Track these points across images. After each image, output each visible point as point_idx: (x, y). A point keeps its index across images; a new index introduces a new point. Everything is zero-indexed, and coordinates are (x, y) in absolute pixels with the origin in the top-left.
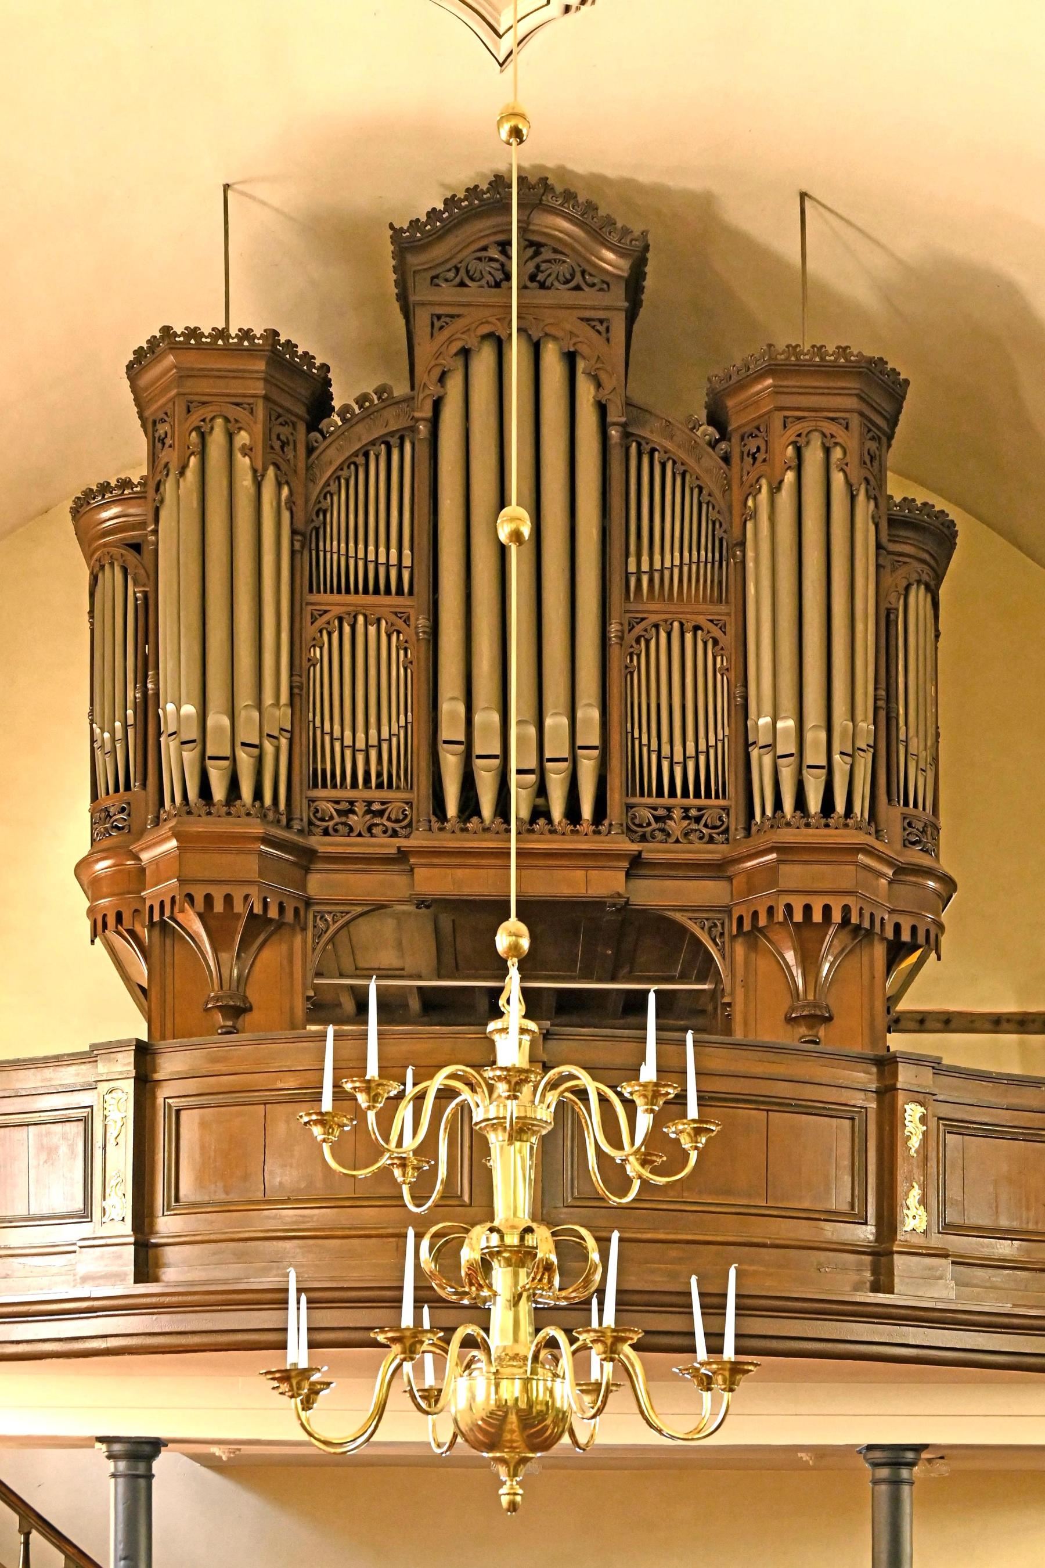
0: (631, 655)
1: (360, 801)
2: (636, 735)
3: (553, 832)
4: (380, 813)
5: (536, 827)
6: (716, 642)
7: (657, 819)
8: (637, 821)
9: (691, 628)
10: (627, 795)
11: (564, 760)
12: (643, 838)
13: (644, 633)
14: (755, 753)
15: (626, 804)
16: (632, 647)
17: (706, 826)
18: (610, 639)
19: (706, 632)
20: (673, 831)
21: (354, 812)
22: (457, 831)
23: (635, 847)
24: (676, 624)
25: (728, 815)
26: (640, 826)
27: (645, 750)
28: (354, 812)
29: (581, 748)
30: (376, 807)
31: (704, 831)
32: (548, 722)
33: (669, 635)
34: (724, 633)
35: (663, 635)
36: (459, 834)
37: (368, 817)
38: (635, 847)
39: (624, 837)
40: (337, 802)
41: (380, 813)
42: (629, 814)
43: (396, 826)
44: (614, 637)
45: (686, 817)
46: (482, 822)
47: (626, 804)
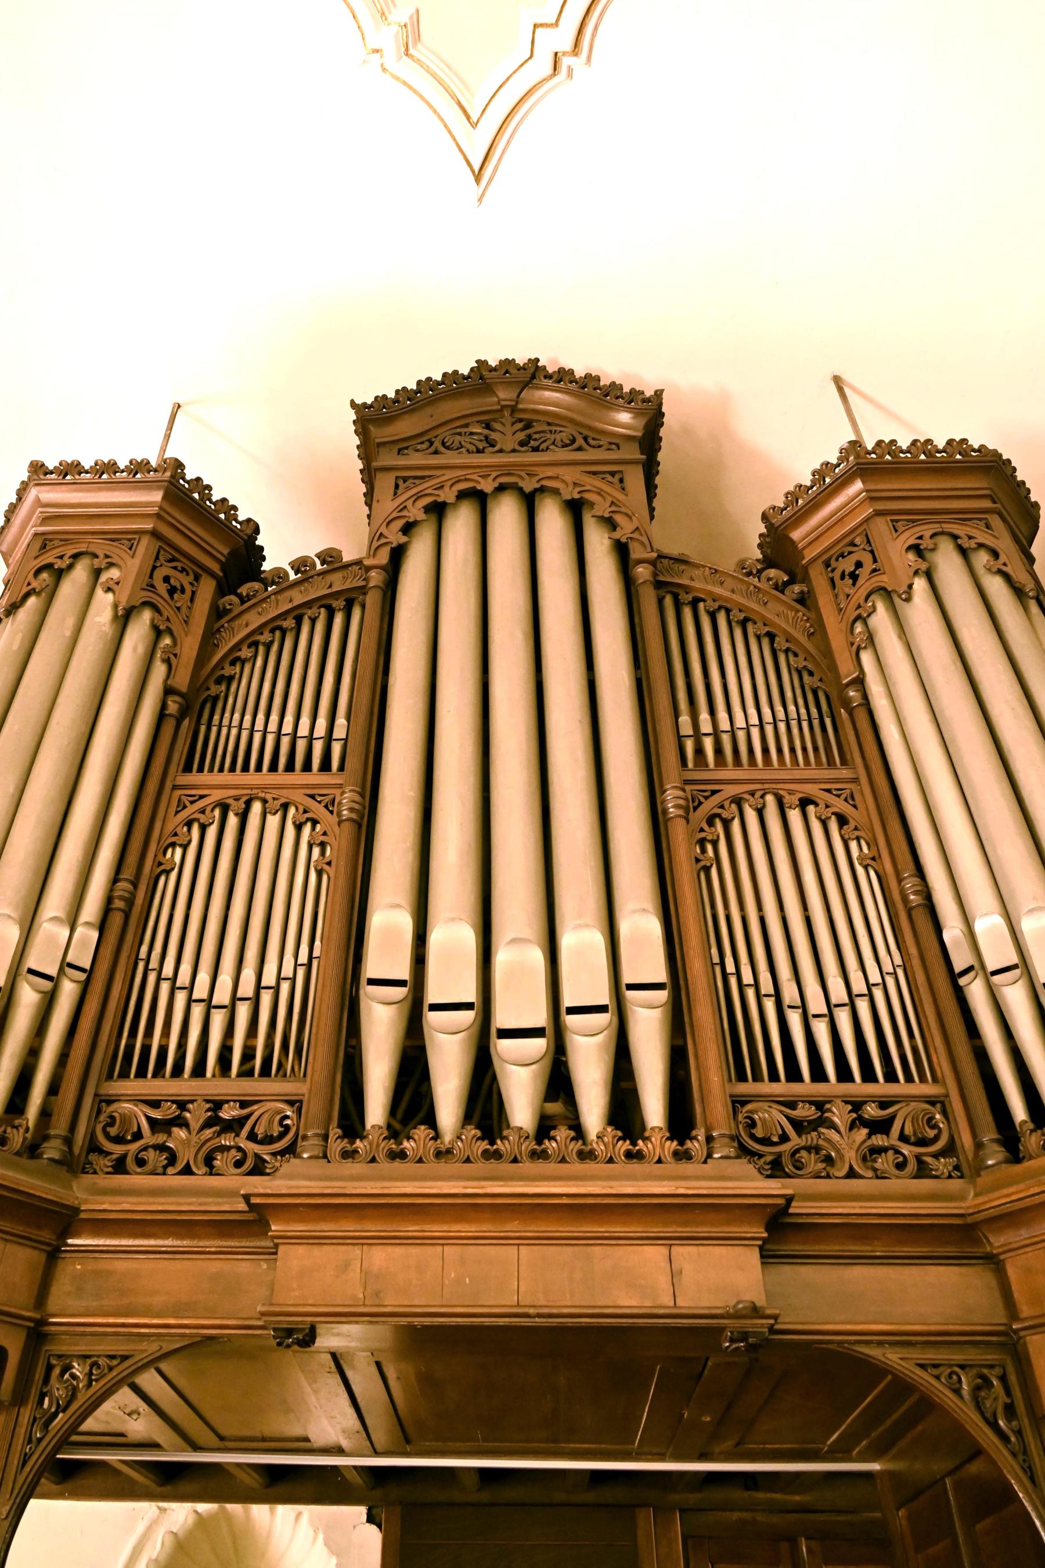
0: (702, 842)
2: (730, 968)
3: (586, 1155)
4: (233, 1126)
5: (551, 1146)
6: (842, 821)
7: (798, 1125)
8: (759, 1132)
9: (798, 803)
10: (730, 1080)
11: (602, 1009)
12: (776, 1169)
13: (719, 811)
14: (976, 992)
15: (731, 1096)
16: (702, 830)
17: (903, 1138)
18: (665, 811)
19: (822, 806)
20: (838, 1151)
21: (185, 1124)
22: (381, 1156)
23: (775, 1187)
24: (770, 799)
25: (944, 1113)
26: (766, 1141)
27: (750, 993)
28: (185, 1124)
29: (631, 987)
30: (228, 1113)
31: (906, 1149)
32: (567, 941)
33: (760, 813)
34: (855, 806)
35: (751, 816)
37: (208, 1132)
38: (775, 1187)
39: (744, 1166)
40: (155, 1104)
41: (233, 1126)
42: (740, 1117)
43: (263, 1151)
44: (672, 807)
45: (862, 1122)
46: (437, 1137)
47: (731, 1096)
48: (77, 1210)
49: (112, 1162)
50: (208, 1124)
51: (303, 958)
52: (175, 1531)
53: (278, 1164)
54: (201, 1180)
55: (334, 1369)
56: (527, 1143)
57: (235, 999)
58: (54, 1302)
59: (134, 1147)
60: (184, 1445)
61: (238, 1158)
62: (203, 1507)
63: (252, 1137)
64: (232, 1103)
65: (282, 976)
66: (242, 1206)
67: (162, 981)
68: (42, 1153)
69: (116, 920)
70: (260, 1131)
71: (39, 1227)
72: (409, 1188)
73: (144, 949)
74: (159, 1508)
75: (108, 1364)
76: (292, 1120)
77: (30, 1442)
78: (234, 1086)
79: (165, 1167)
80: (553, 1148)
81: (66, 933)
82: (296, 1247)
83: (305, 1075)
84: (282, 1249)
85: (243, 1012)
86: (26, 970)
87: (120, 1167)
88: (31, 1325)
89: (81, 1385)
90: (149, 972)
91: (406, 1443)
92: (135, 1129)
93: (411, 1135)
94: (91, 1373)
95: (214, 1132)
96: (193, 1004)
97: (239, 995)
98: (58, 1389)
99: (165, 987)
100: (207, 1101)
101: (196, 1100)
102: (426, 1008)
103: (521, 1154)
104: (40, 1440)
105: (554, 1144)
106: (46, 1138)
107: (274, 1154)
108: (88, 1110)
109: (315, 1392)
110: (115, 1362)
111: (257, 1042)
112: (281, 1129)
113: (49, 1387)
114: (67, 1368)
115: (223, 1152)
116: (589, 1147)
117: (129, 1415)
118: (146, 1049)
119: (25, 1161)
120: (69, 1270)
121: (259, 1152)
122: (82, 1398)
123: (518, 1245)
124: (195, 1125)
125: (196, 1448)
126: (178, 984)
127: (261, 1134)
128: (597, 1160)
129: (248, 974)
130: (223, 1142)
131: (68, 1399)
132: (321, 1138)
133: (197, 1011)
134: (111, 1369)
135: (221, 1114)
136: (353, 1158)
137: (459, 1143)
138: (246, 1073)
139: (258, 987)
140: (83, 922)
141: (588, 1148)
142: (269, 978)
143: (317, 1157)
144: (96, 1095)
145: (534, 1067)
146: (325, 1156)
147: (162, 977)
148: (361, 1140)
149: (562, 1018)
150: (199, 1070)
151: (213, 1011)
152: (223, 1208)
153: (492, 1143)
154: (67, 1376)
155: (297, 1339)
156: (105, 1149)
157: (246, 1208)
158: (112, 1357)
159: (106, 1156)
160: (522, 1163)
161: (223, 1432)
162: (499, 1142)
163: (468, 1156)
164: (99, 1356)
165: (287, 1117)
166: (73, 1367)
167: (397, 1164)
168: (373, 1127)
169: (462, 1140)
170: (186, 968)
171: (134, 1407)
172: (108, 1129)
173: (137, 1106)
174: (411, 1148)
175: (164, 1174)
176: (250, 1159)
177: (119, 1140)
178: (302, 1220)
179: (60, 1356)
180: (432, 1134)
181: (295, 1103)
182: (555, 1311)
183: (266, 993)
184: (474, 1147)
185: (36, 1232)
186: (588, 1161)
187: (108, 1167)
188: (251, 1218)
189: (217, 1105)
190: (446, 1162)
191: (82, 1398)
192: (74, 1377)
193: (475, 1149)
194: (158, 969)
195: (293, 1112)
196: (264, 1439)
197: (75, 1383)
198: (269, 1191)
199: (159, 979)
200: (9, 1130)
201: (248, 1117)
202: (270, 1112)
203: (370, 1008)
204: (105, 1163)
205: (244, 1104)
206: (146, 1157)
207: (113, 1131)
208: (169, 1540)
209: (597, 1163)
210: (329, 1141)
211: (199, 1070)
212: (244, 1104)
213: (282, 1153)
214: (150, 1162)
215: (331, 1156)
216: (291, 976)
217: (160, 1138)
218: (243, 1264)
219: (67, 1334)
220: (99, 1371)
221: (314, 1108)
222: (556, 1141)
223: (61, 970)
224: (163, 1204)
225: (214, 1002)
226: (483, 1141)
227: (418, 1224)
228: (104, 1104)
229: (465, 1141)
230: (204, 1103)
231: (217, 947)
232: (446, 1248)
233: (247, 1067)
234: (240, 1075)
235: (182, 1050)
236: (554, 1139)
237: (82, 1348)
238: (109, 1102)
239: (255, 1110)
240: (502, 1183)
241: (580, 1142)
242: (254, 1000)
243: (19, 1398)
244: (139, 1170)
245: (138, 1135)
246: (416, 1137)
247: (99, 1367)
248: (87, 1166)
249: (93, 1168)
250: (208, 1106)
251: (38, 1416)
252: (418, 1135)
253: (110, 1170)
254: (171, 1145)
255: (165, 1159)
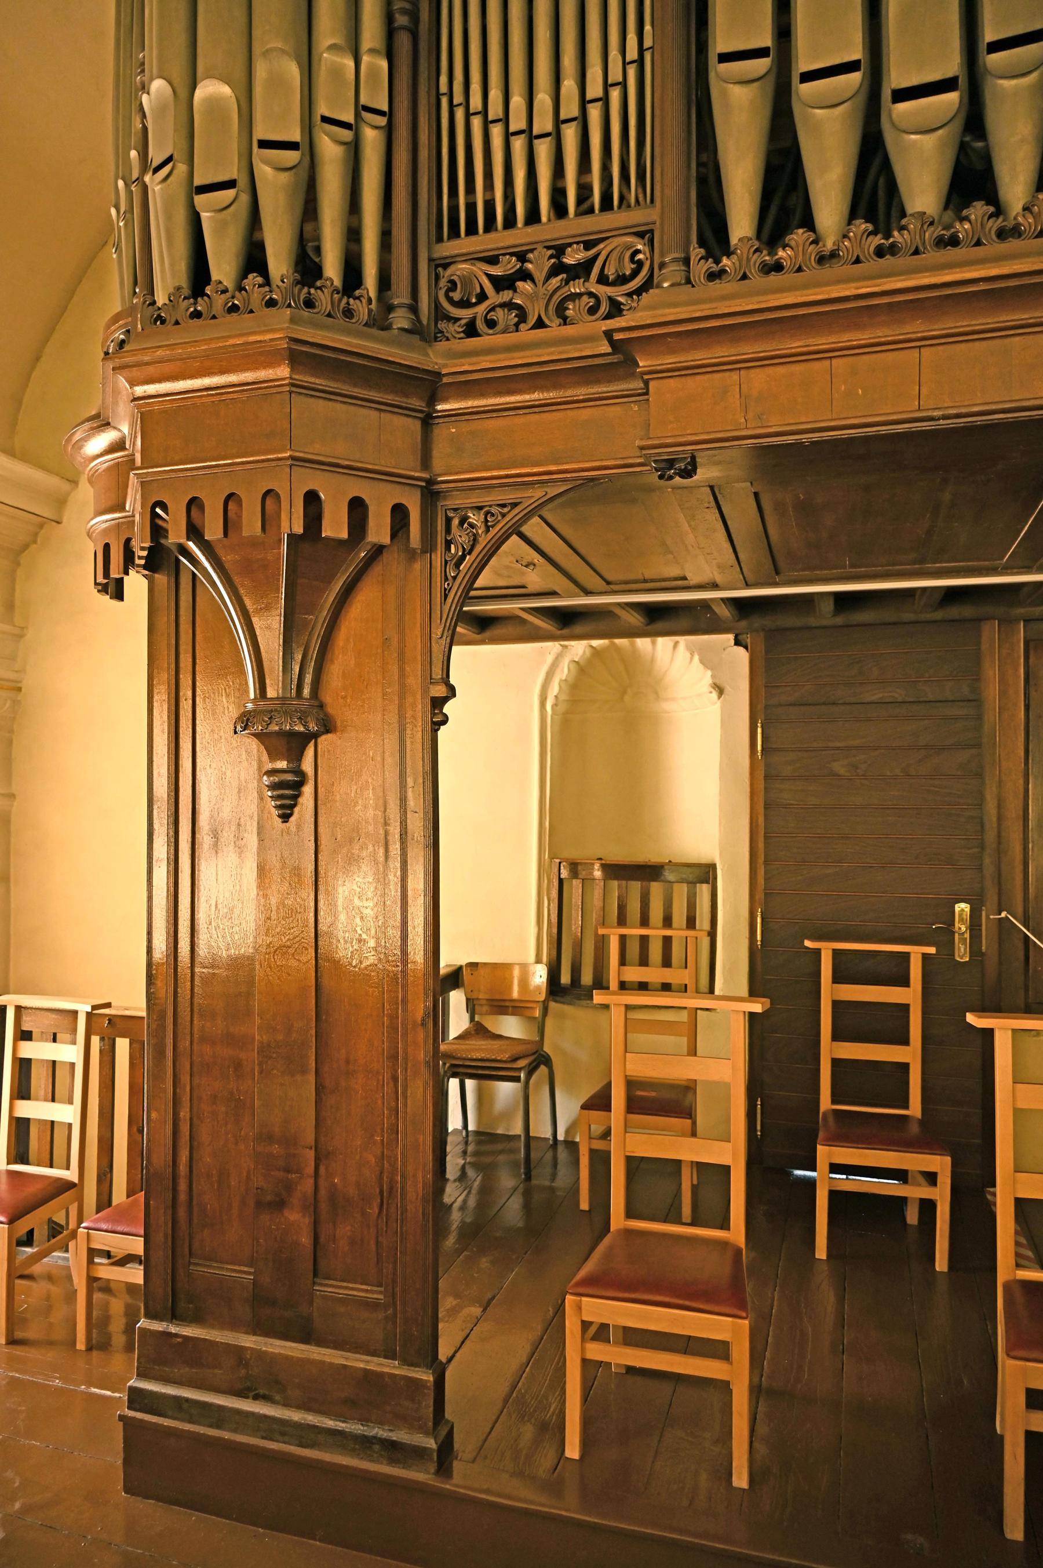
1: (539, 247)
4: (583, 269)
21: (526, 276)
22: (753, 272)
28: (526, 276)
30: (572, 258)
36: (757, 280)
37: (555, 281)
40: (493, 260)
41: (583, 269)
43: (617, 292)
48: (438, 375)
49: (462, 327)
50: (554, 272)
51: (632, 53)
52: (577, 660)
53: (634, 305)
54: (555, 329)
55: (713, 504)
56: (932, 229)
57: (559, 122)
58: (438, 463)
59: (481, 309)
60: (577, 590)
61: (591, 304)
62: (595, 643)
63: (602, 280)
64: (575, 246)
65: (610, 81)
66: (606, 348)
67: (472, 117)
68: (391, 324)
69: (403, 41)
70: (611, 272)
71: (406, 396)
72: (790, 299)
73: (444, 79)
74: (561, 645)
75: (500, 513)
76: (645, 254)
77: (446, 579)
78: (574, 225)
79: (517, 325)
80: (966, 230)
81: (351, 64)
82: (667, 380)
83: (652, 201)
84: (652, 384)
85: (570, 135)
86: (319, 118)
87: (471, 331)
88: (424, 484)
89: (480, 532)
90: (455, 108)
91: (776, 573)
92: (478, 290)
93: (787, 242)
94: (486, 521)
95: (562, 280)
96: (512, 138)
97: (563, 116)
98: (460, 536)
99: (476, 122)
100: (548, 248)
101: (535, 249)
102: (795, 78)
103: (924, 243)
104: (454, 578)
105: (967, 226)
106: (390, 308)
107: (629, 295)
108: (426, 277)
109: (694, 529)
110: (506, 510)
111: (592, 178)
112: (633, 266)
113: (452, 536)
114: (463, 520)
115: (574, 301)
116: (1013, 223)
117: (526, 566)
118: (471, 207)
119: (374, 331)
120: (443, 434)
121: (612, 294)
122: (483, 541)
123: (920, 347)
124: (540, 276)
125: (588, 593)
126: (490, 118)
127: (613, 274)
128: (1022, 238)
129: (569, 85)
130: (573, 291)
131: (471, 543)
132: (681, 263)
133: (518, 145)
134: (504, 515)
135: (565, 260)
136: (720, 279)
137: (846, 243)
138: (585, 208)
139: (584, 103)
140: (366, 49)
141: (1010, 224)
142: (595, 90)
143: (679, 284)
144: (431, 260)
145: (940, 132)
146: (688, 281)
147: (471, 111)
148: (728, 257)
149: (981, 62)
150: (533, 216)
151: (536, 142)
152: (584, 354)
153: (888, 235)
154: (466, 525)
155: (680, 469)
156: (452, 315)
157: (609, 350)
158: (503, 506)
159: (454, 323)
160: (924, 253)
161: (609, 578)
162: (896, 233)
163: (858, 256)
164: (490, 506)
165: (638, 252)
166: (470, 517)
167: (774, 278)
168: (740, 240)
169: (849, 239)
170: (495, 94)
171: (530, 560)
172: (451, 294)
173: (472, 264)
174: (788, 257)
175: (517, 331)
176: (605, 304)
177: (464, 304)
178: (673, 352)
179: (455, 510)
180: (812, 237)
181: (645, 234)
182: (964, 410)
183: (595, 108)
184: (865, 244)
185: (405, 400)
186: (1010, 239)
187: (459, 333)
188: (615, 361)
189: (559, 251)
190: (830, 267)
191: (483, 541)
192: (472, 526)
193: (866, 247)
194: (464, 103)
195: (645, 244)
196: (645, 581)
197: (474, 531)
198: (633, 324)
199: (468, 115)
200: (351, 301)
201: (595, 258)
202: (619, 248)
203: (724, 94)
204: (454, 329)
205: (588, 245)
206: (495, 318)
207: (456, 296)
208: (573, 666)
209: (1023, 240)
210: (692, 263)
211: (533, 216)
212: (588, 245)
213: (639, 291)
214: (501, 322)
215: (695, 281)
216: (621, 80)
217: (506, 296)
218: (613, 409)
219: (458, 490)
220: (494, 518)
221: (668, 233)
222: (970, 222)
223: (357, 115)
224: (523, 357)
225: (536, 131)
226: (876, 235)
227: (799, 340)
228: (440, 269)
229: (853, 240)
230: (545, 250)
231: (526, 63)
232: (834, 361)
233: (585, 206)
234: (578, 214)
235: (510, 200)
236: (967, 219)
237: (475, 499)
238: (445, 266)
239: (603, 249)
240: (903, 277)
241: (1001, 219)
242: (580, 120)
243: (428, 546)
244: (491, 332)
245: (482, 297)
246: (793, 243)
247: (493, 515)
248: (439, 335)
249: (445, 336)
250: (550, 252)
251: (448, 559)
252: (795, 241)
253: (462, 335)
254: (519, 302)
255: (515, 316)
